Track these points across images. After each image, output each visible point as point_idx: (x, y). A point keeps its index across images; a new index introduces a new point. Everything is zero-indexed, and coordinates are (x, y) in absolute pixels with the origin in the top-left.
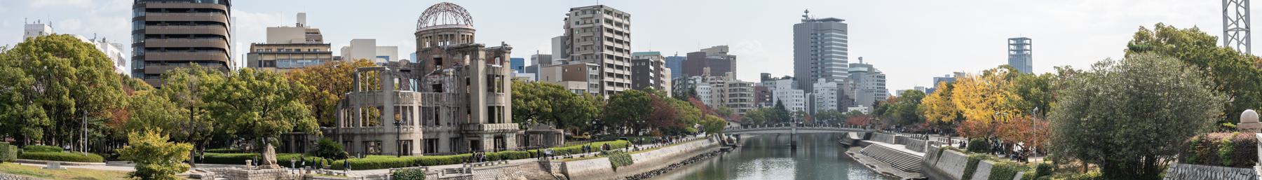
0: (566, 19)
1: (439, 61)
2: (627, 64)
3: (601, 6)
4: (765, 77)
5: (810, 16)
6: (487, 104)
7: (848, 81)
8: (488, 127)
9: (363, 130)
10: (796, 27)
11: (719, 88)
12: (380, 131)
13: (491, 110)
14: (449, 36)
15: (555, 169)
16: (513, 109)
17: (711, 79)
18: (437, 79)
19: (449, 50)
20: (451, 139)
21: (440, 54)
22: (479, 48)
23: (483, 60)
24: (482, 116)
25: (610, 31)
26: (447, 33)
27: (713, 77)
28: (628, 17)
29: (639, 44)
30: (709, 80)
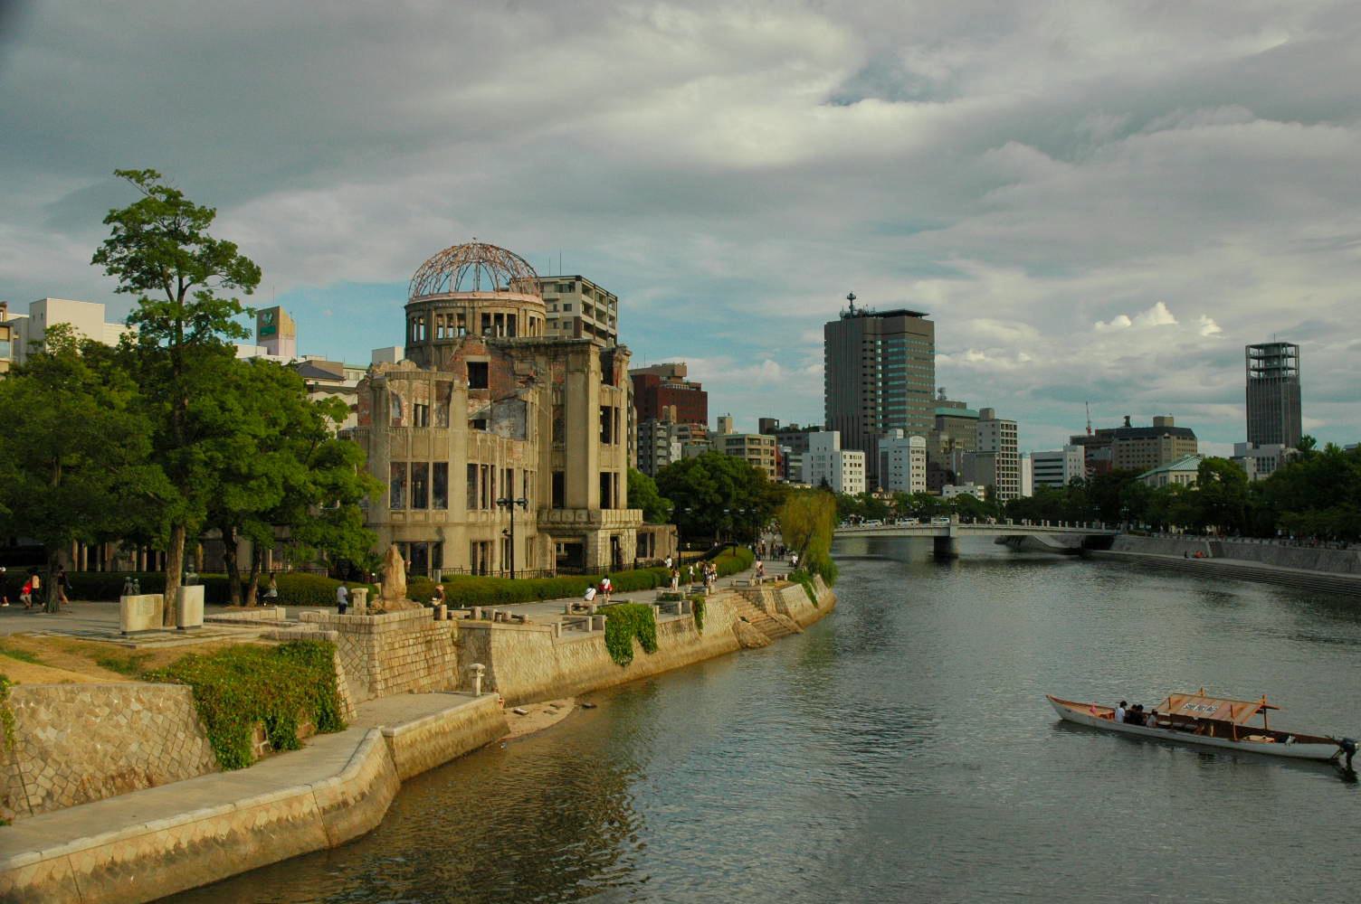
3: (578, 278)
5: (859, 305)
6: (599, 466)
7: (938, 436)
9: (395, 516)
10: (830, 329)
14: (505, 318)
15: (769, 603)
17: (680, 430)
20: (527, 539)
22: (591, 347)
23: (596, 373)
25: (589, 327)
26: (501, 311)
27: (685, 425)
28: (613, 301)
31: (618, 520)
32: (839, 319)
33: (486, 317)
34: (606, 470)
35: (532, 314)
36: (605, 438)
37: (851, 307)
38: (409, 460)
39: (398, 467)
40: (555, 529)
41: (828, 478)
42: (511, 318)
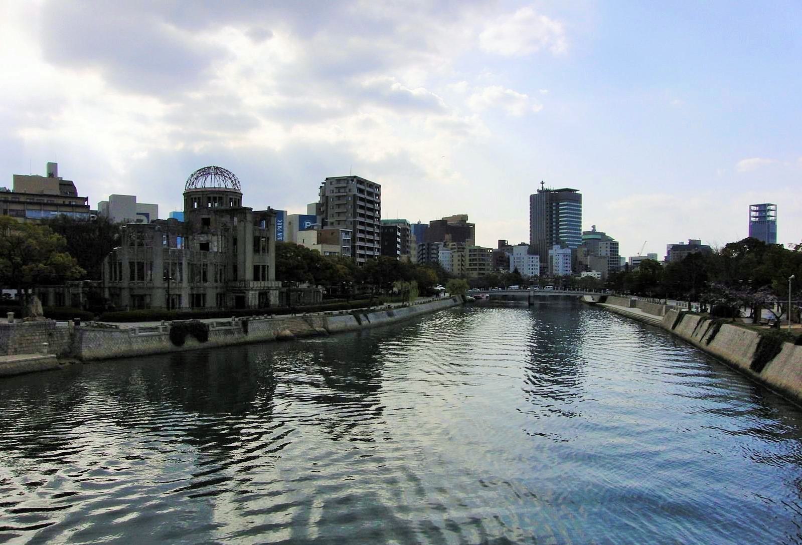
0: (321, 187)
1: (206, 222)
2: (377, 231)
3: (355, 177)
4: (502, 243)
6: (253, 262)
8: (252, 284)
11: (460, 253)
12: (151, 285)
13: (256, 268)
14: (217, 199)
16: (277, 267)
17: (452, 245)
18: (203, 239)
19: (216, 212)
20: (217, 294)
21: (208, 215)
22: (247, 211)
23: (251, 222)
24: (249, 274)
25: (362, 199)
26: (215, 195)
28: (378, 187)
29: (388, 212)
30: (450, 246)
31: (262, 286)
32: (537, 193)
33: (209, 198)
34: (258, 264)
35: (231, 197)
36: (256, 249)
37: (542, 187)
38: (136, 261)
39: (132, 264)
40: (233, 290)
41: (518, 267)
42: (221, 198)
